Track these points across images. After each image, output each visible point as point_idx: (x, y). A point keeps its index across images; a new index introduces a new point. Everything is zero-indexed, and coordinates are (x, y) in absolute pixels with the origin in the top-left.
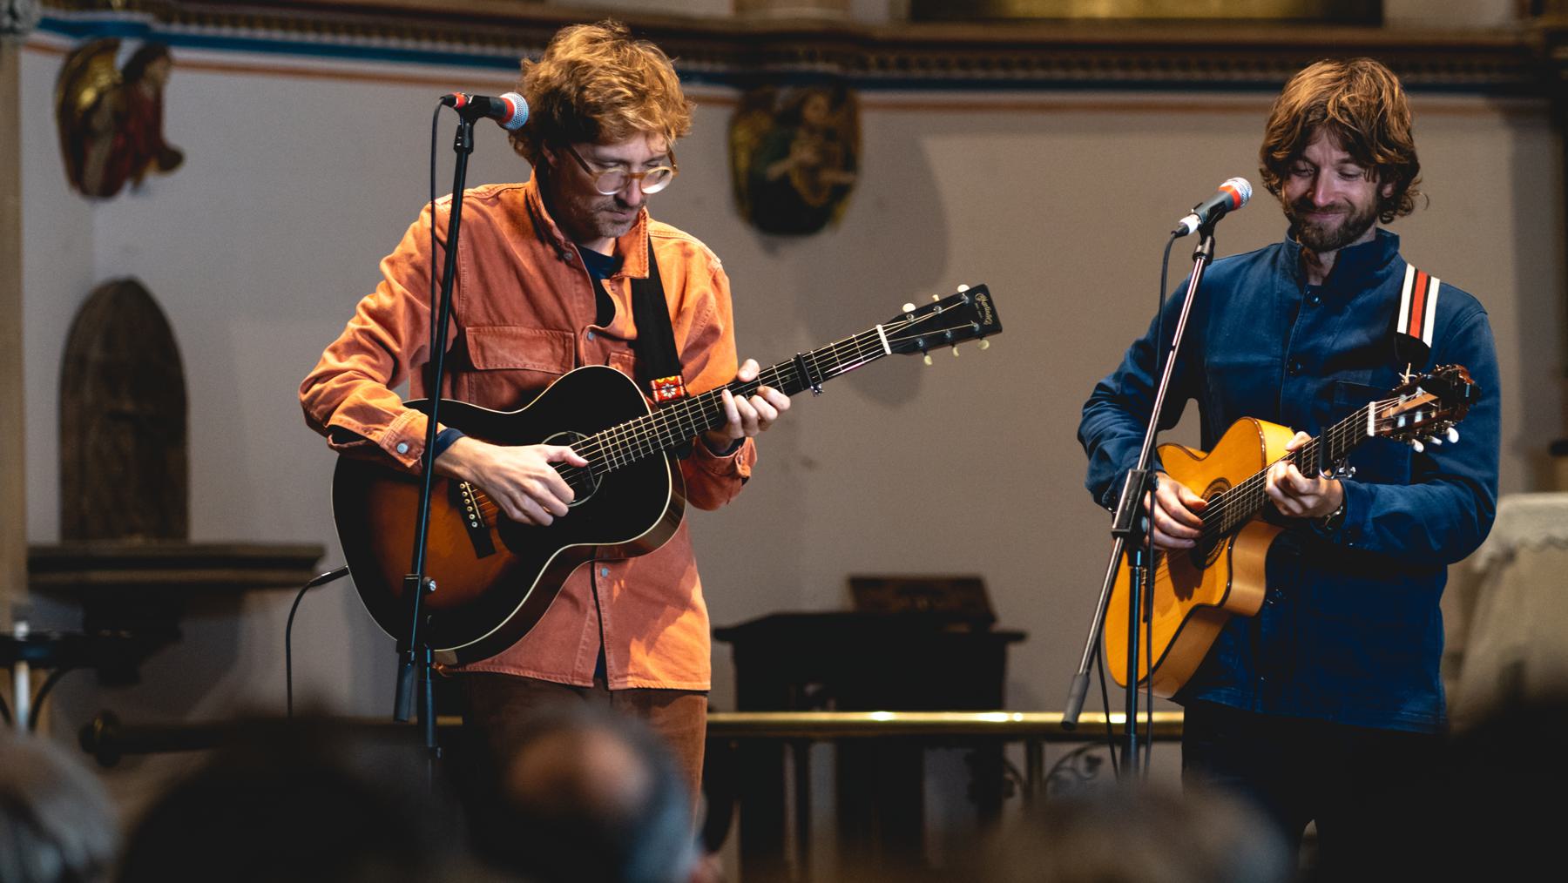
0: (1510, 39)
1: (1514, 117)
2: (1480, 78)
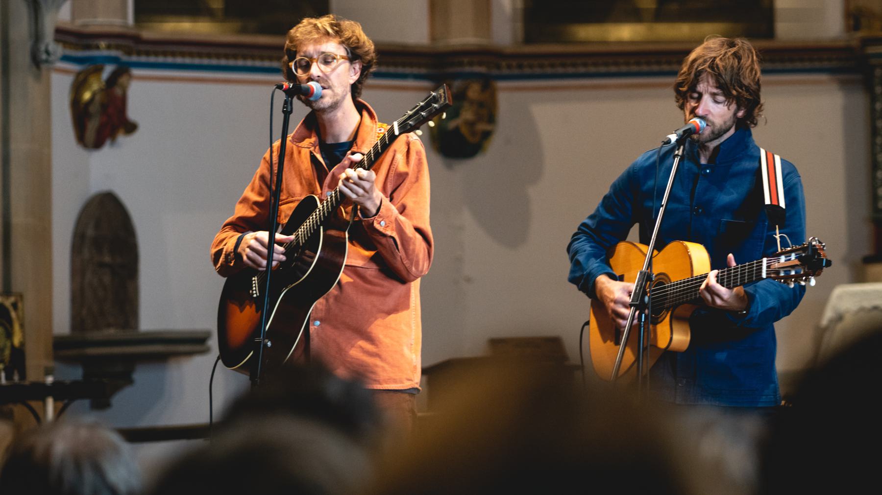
0: (841, 44)
1: (845, 85)
2: (826, 64)
